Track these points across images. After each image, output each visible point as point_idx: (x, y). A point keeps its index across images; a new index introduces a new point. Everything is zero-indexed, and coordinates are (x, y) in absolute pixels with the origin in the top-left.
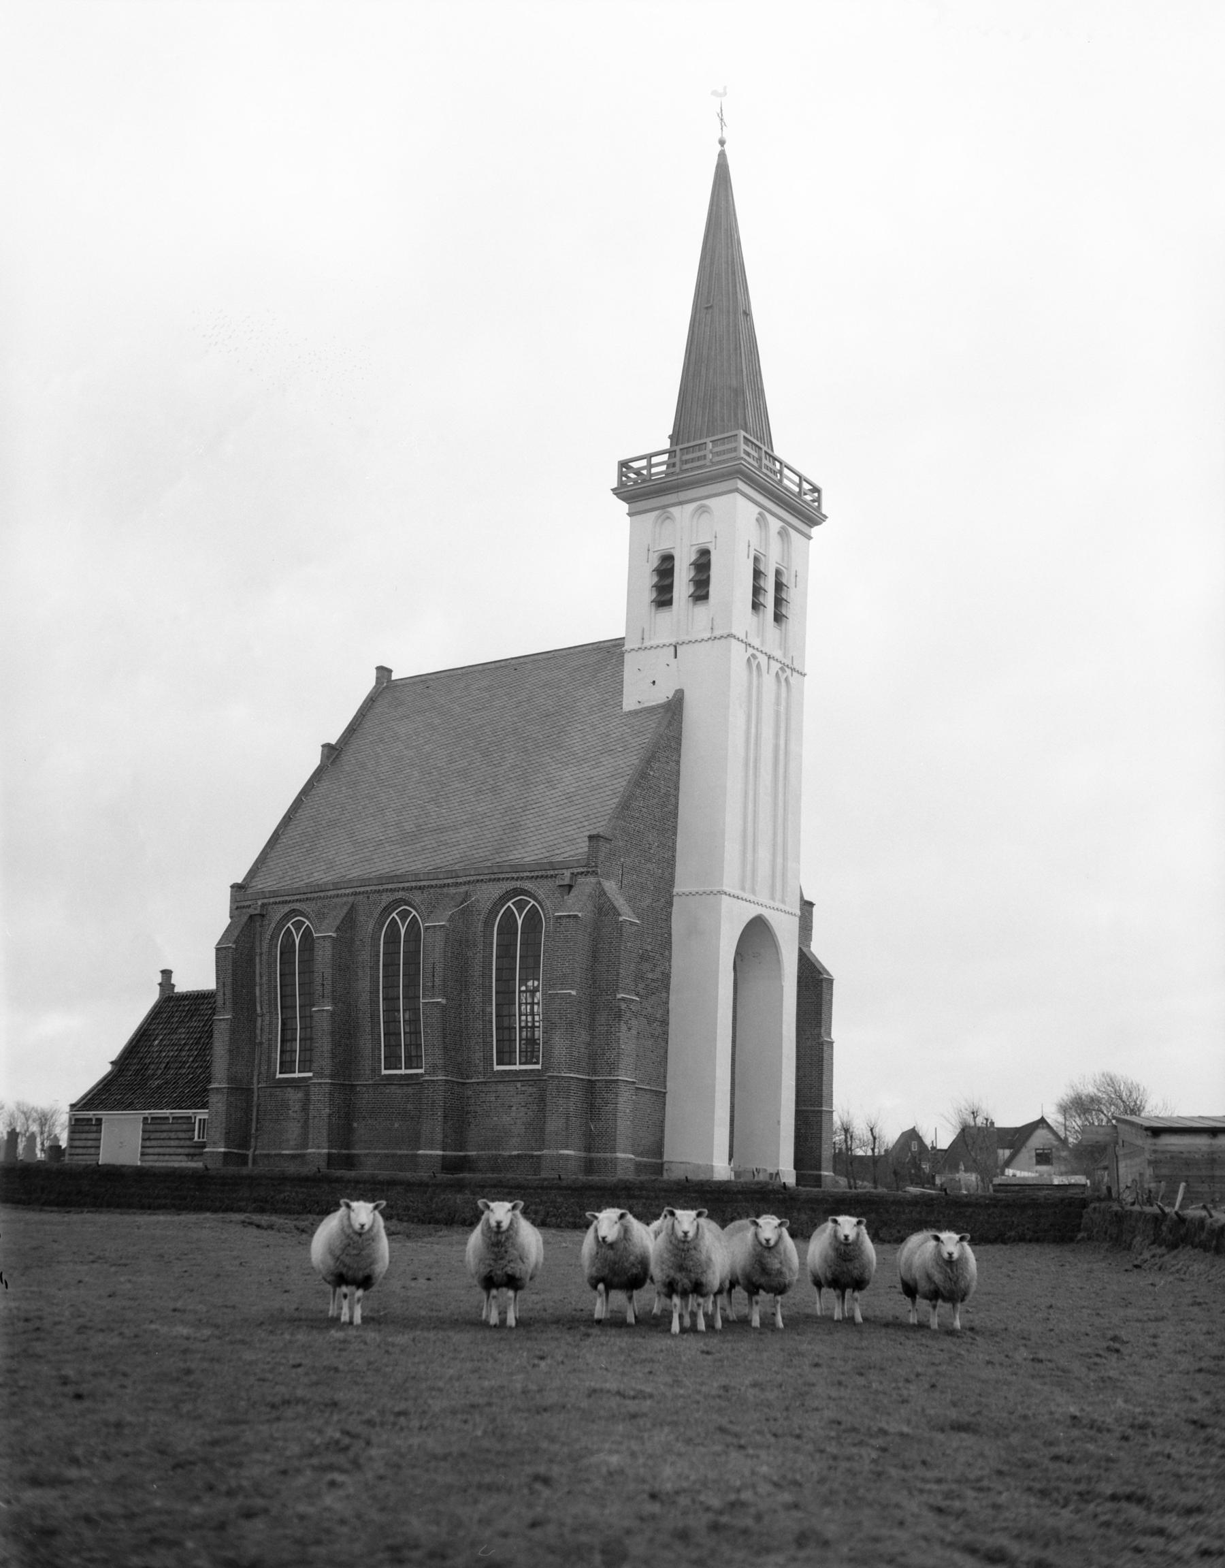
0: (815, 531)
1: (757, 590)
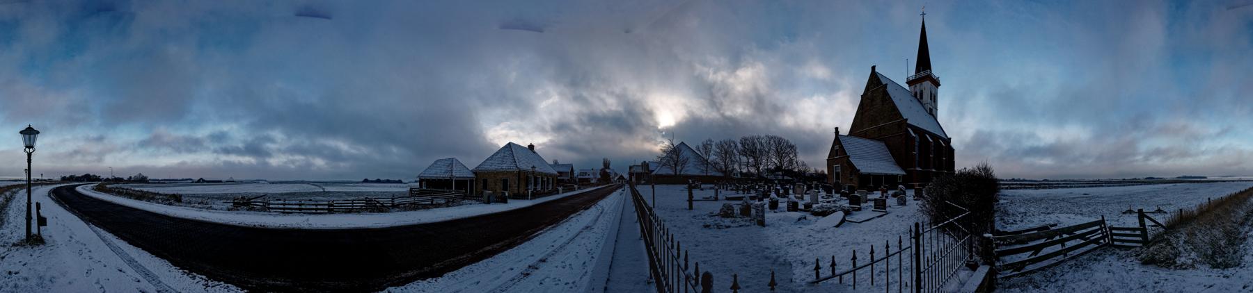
1: (931, 96)
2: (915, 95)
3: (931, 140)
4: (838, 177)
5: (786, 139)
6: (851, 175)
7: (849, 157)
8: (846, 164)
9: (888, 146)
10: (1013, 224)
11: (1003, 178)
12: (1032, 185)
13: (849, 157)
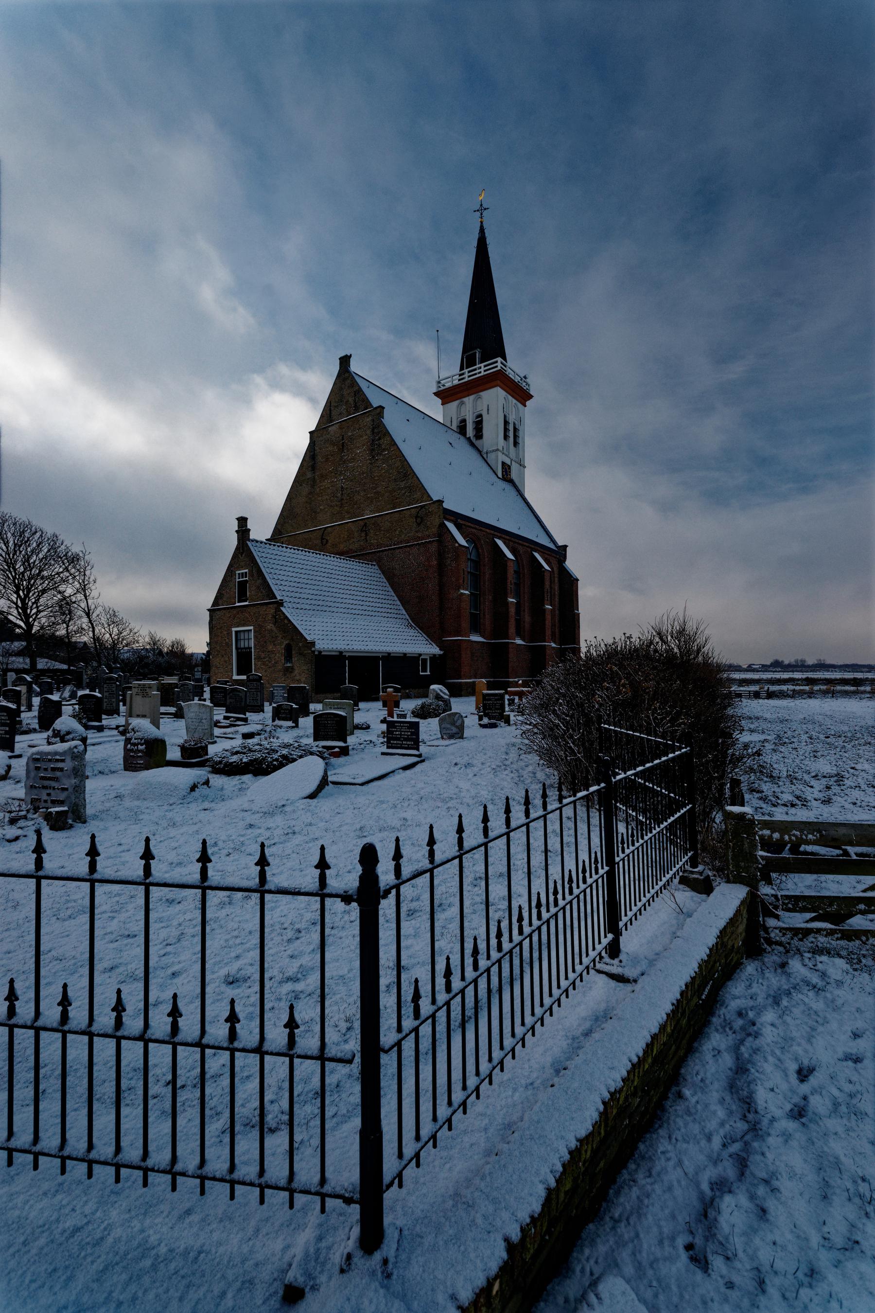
0: (528, 403)
1: (506, 430)
2: (462, 429)
3: (510, 555)
4: (244, 666)
5: (49, 531)
6: (288, 657)
7: (280, 603)
8: (271, 626)
9: (390, 577)
10: (793, 805)
11: (735, 662)
12: (856, 682)
13: (280, 603)
